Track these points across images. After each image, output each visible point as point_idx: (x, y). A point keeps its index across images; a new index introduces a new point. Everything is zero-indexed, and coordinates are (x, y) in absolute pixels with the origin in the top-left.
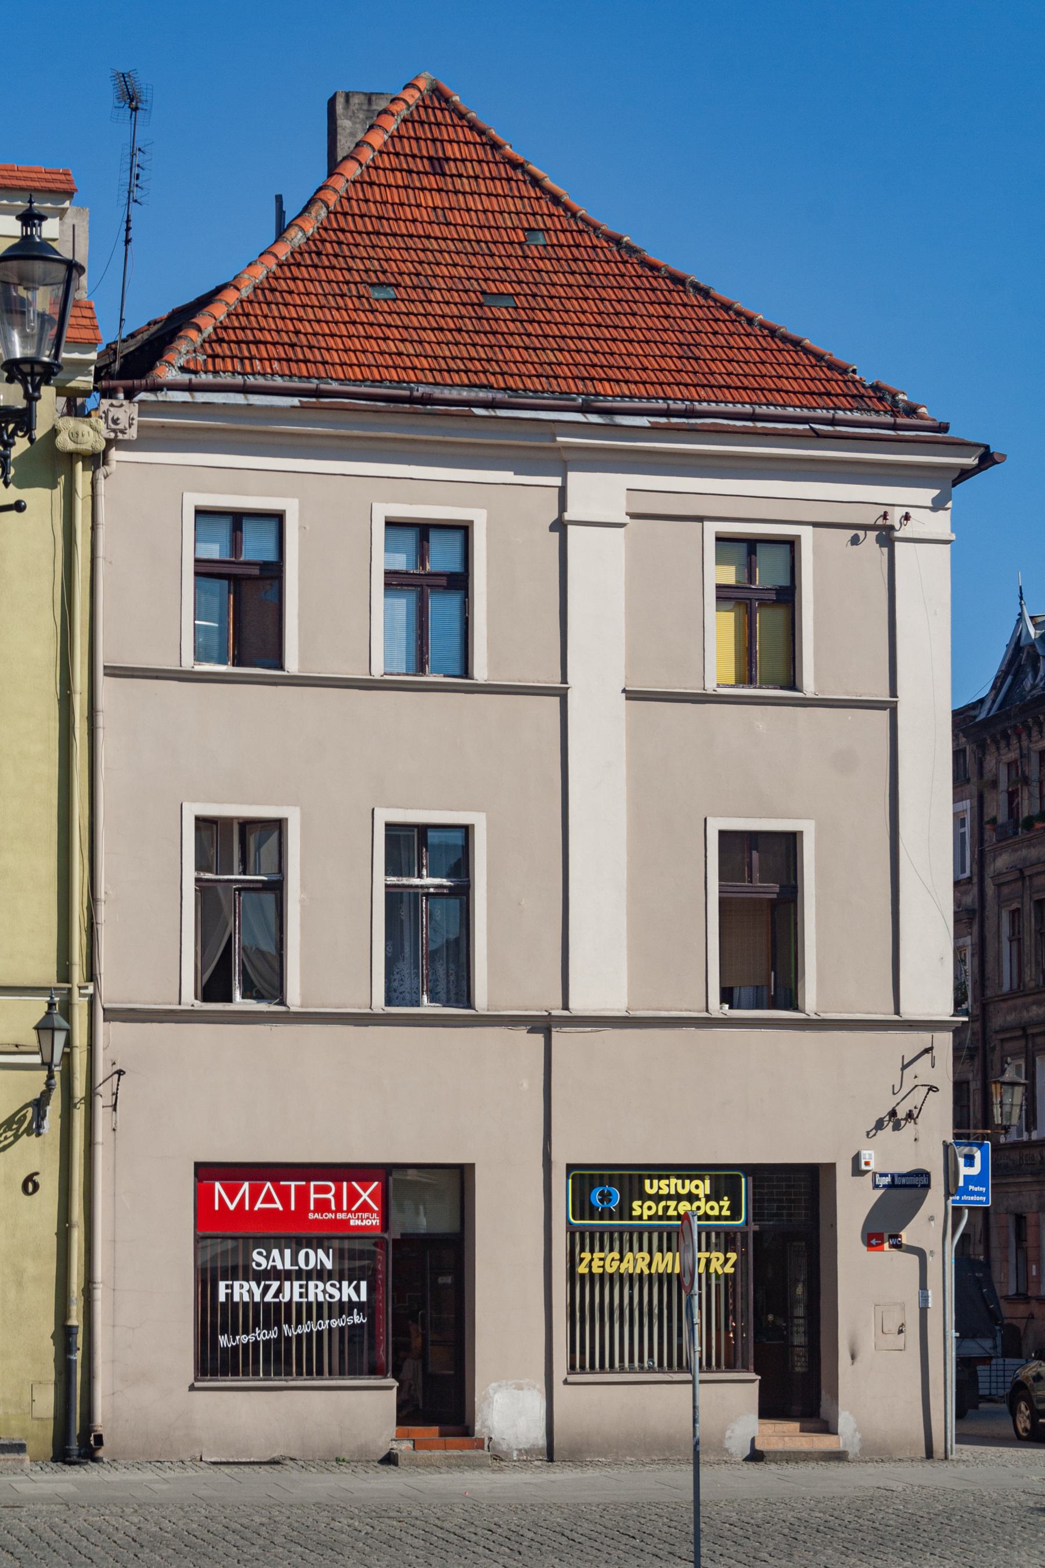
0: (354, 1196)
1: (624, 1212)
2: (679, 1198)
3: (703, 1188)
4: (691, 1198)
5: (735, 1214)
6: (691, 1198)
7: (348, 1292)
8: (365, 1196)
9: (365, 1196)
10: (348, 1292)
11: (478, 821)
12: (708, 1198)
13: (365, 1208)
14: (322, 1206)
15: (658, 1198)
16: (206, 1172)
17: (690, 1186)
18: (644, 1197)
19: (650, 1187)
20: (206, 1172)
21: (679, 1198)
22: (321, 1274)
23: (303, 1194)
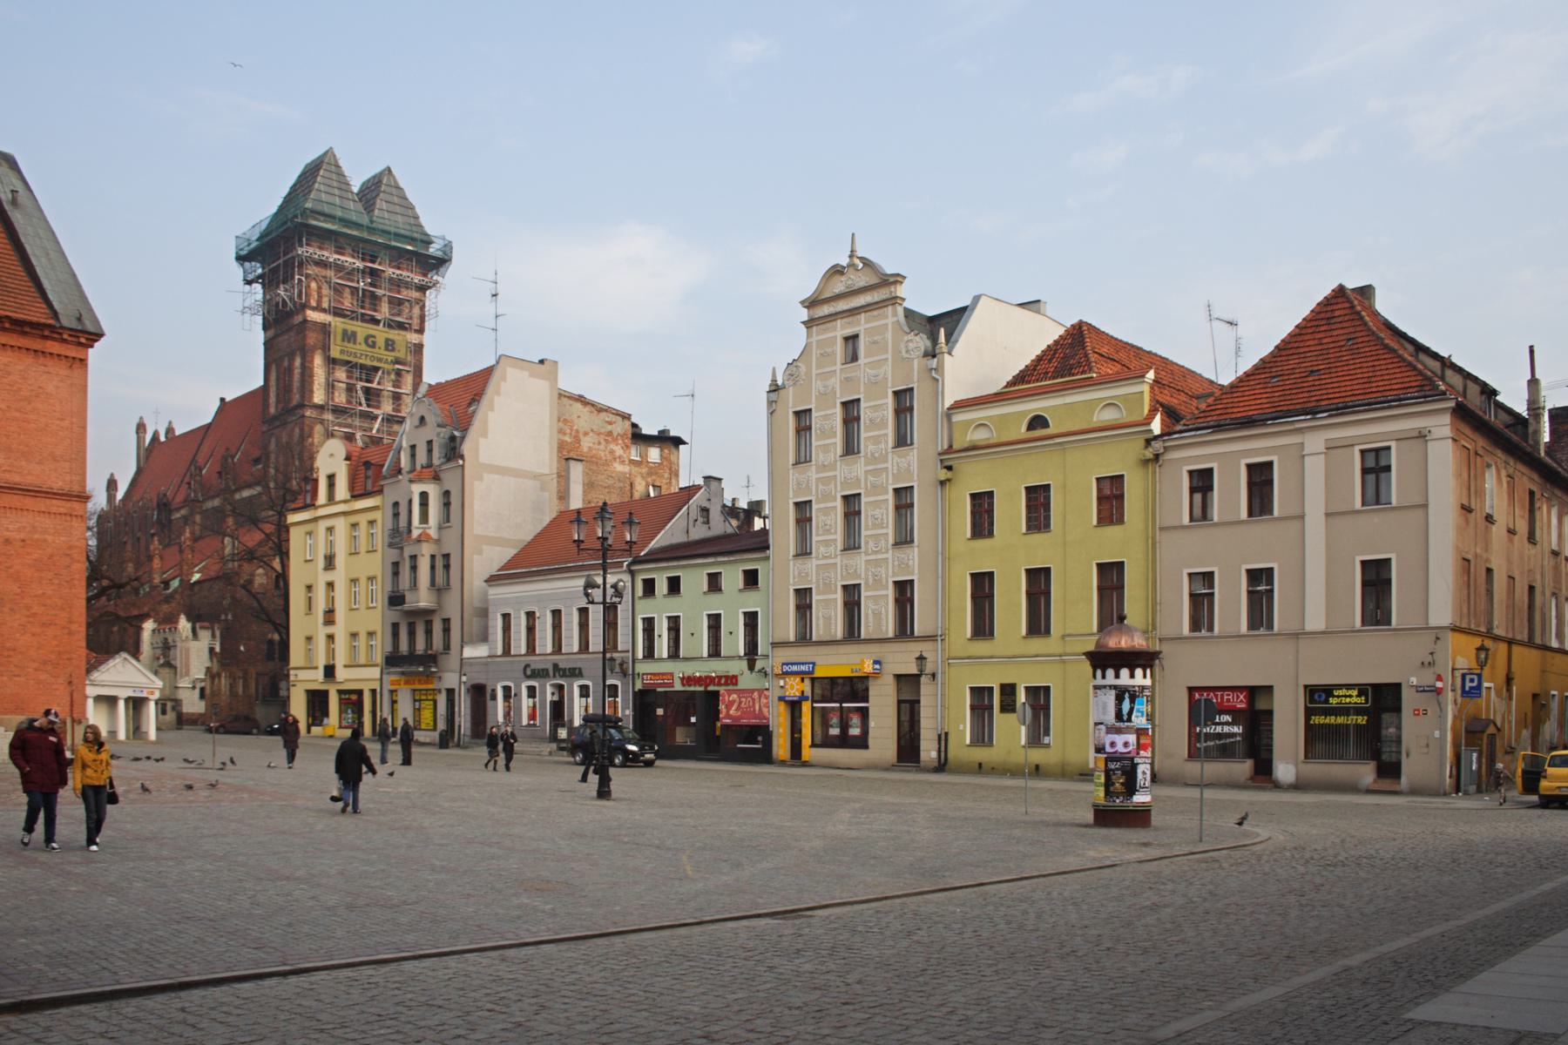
0: (1238, 697)
1: (1327, 701)
2: (1346, 696)
3: (1355, 693)
4: (1350, 696)
5: (1367, 702)
6: (1350, 696)
7: (1236, 729)
8: (1242, 697)
9: (1242, 697)
10: (1236, 729)
11: (1359, 559)
12: (1357, 696)
13: (1241, 701)
14: (1228, 700)
15: (1338, 697)
16: (1191, 690)
17: (1350, 692)
18: (1334, 696)
19: (1336, 693)
20: (1191, 690)
21: (1346, 696)
22: (1227, 723)
23: (1222, 696)
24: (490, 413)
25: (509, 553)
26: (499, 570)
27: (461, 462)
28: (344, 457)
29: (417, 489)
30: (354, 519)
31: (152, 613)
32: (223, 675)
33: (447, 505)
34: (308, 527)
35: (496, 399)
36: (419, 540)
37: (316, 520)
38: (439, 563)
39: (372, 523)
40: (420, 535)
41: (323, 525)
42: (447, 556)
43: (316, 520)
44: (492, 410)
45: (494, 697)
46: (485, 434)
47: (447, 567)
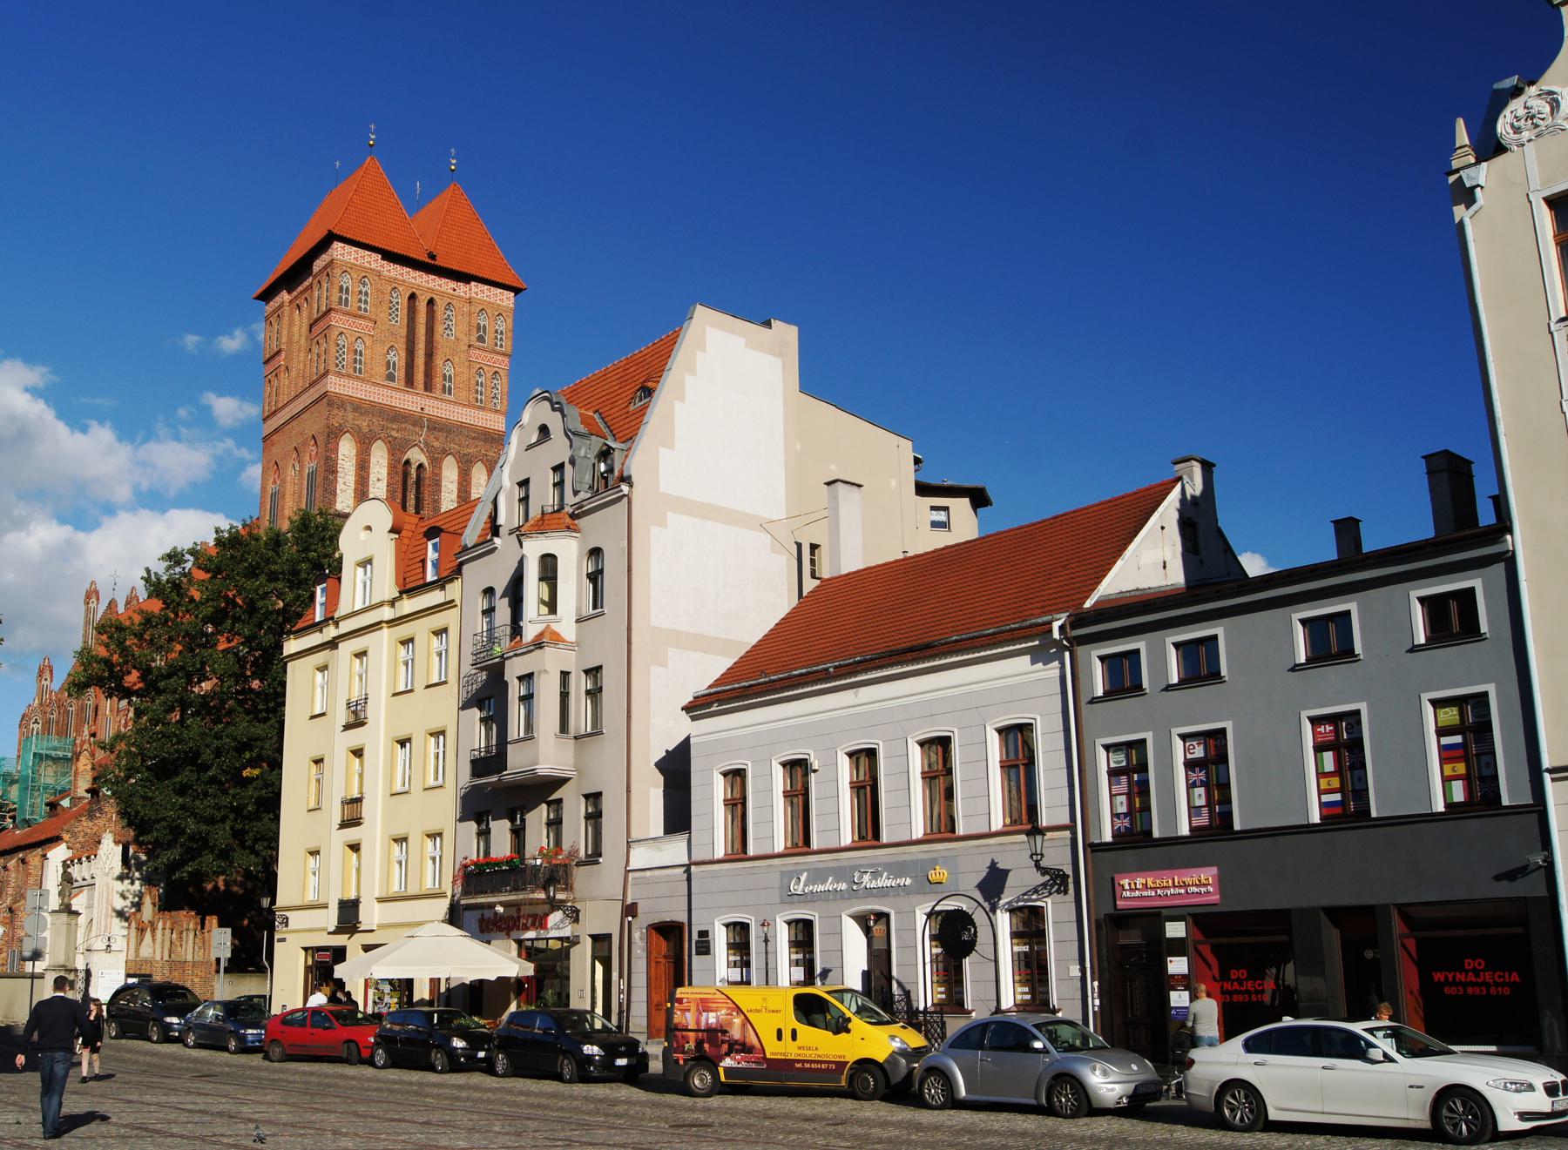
24: (677, 403)
25: (722, 664)
26: (710, 687)
27: (625, 488)
28: (389, 527)
29: (534, 548)
30: (404, 630)
31: (66, 836)
32: (160, 925)
33: (595, 577)
34: (319, 658)
35: (689, 380)
36: (538, 644)
37: (332, 644)
38: (580, 684)
39: (441, 632)
40: (541, 635)
41: (346, 648)
42: (594, 672)
43: (332, 644)
44: (682, 399)
45: (704, 948)
46: (669, 443)
47: (594, 694)
